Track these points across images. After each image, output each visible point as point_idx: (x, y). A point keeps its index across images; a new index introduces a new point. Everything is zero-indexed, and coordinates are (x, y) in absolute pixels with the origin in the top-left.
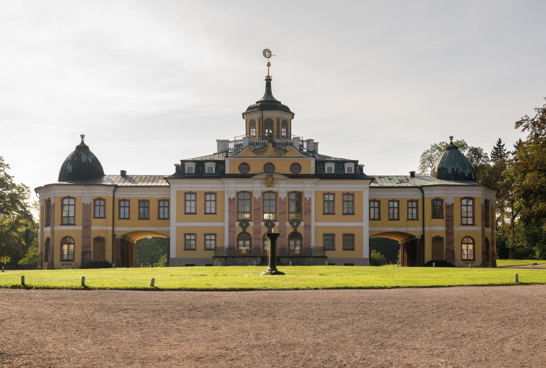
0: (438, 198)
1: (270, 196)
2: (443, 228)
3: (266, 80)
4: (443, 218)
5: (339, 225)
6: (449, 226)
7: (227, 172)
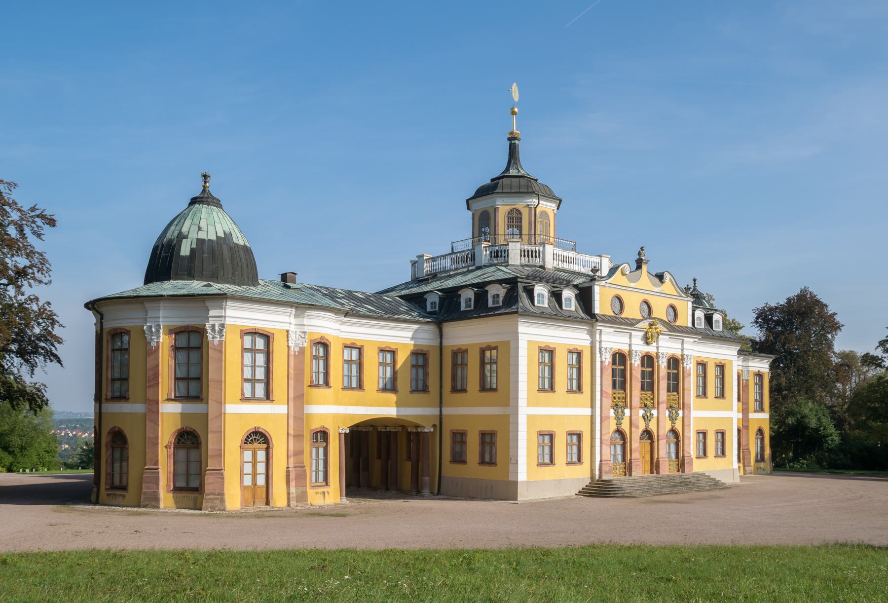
7: (597, 310)
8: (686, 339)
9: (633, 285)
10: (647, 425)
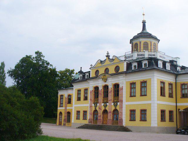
1: (106, 87)
3: (143, 22)
5: (138, 103)
8: (119, 77)
9: (103, 65)
10: (105, 109)
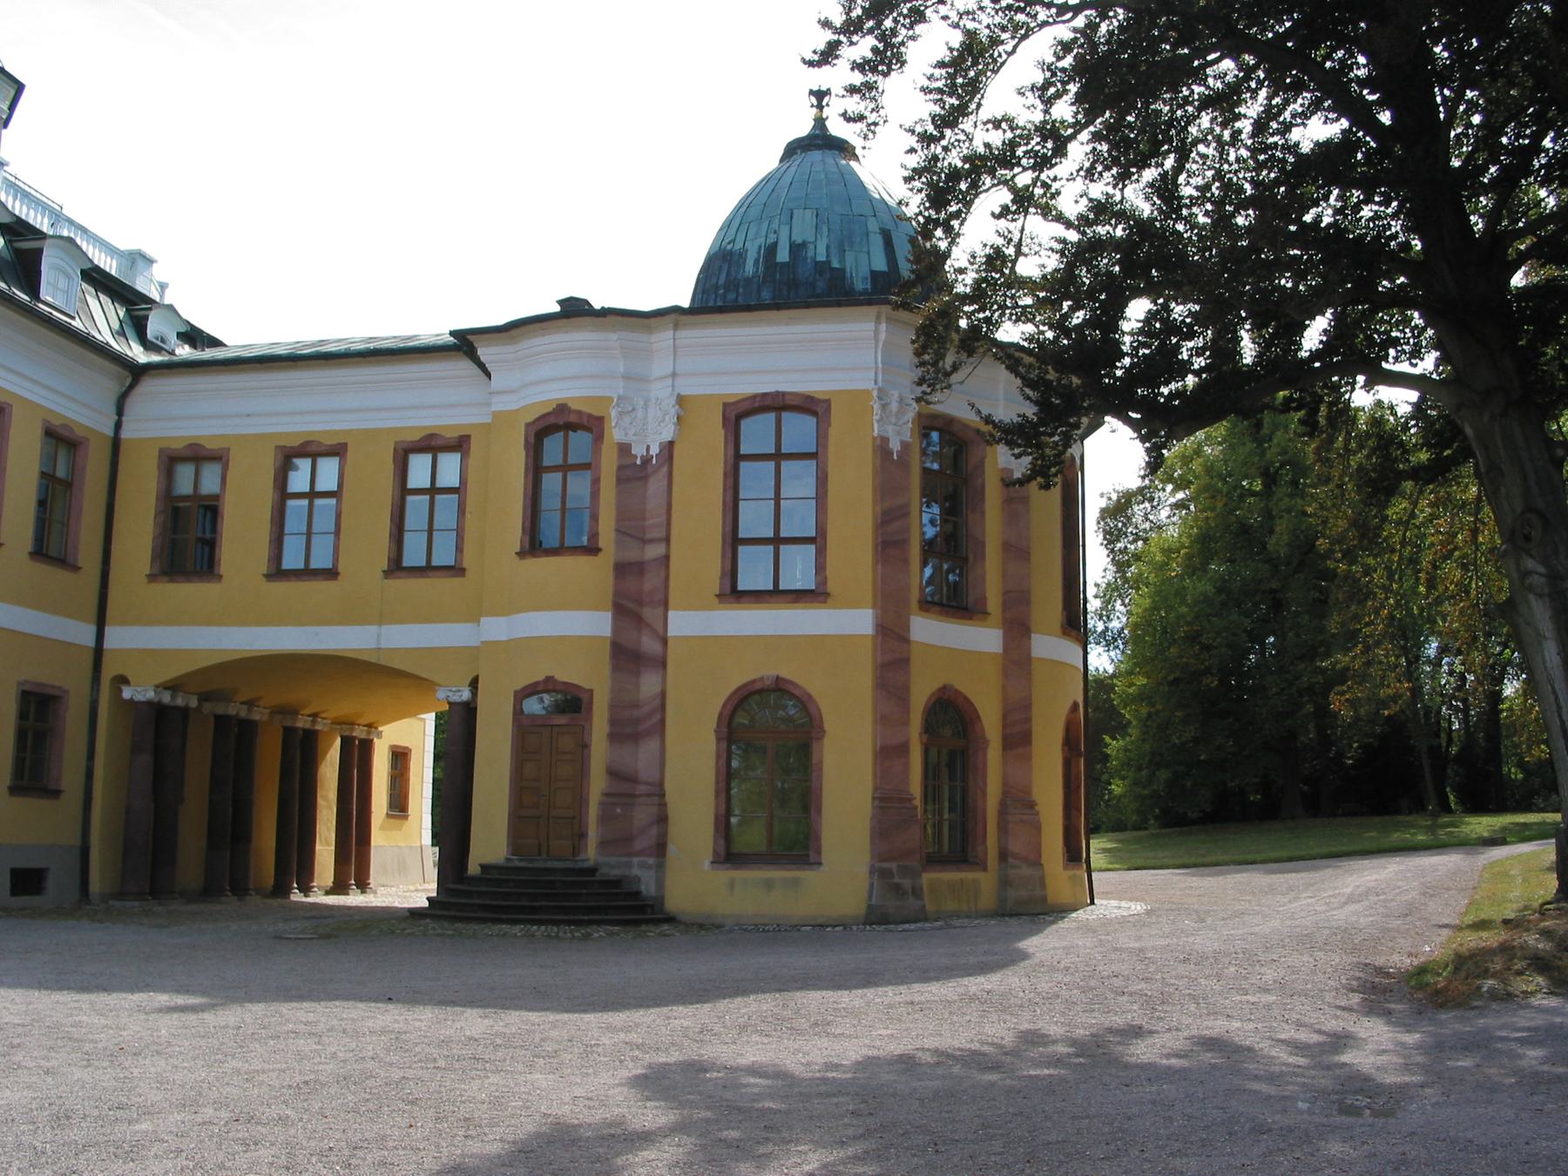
0: (562, 408)
2: (597, 624)
4: (592, 550)
6: (636, 599)
